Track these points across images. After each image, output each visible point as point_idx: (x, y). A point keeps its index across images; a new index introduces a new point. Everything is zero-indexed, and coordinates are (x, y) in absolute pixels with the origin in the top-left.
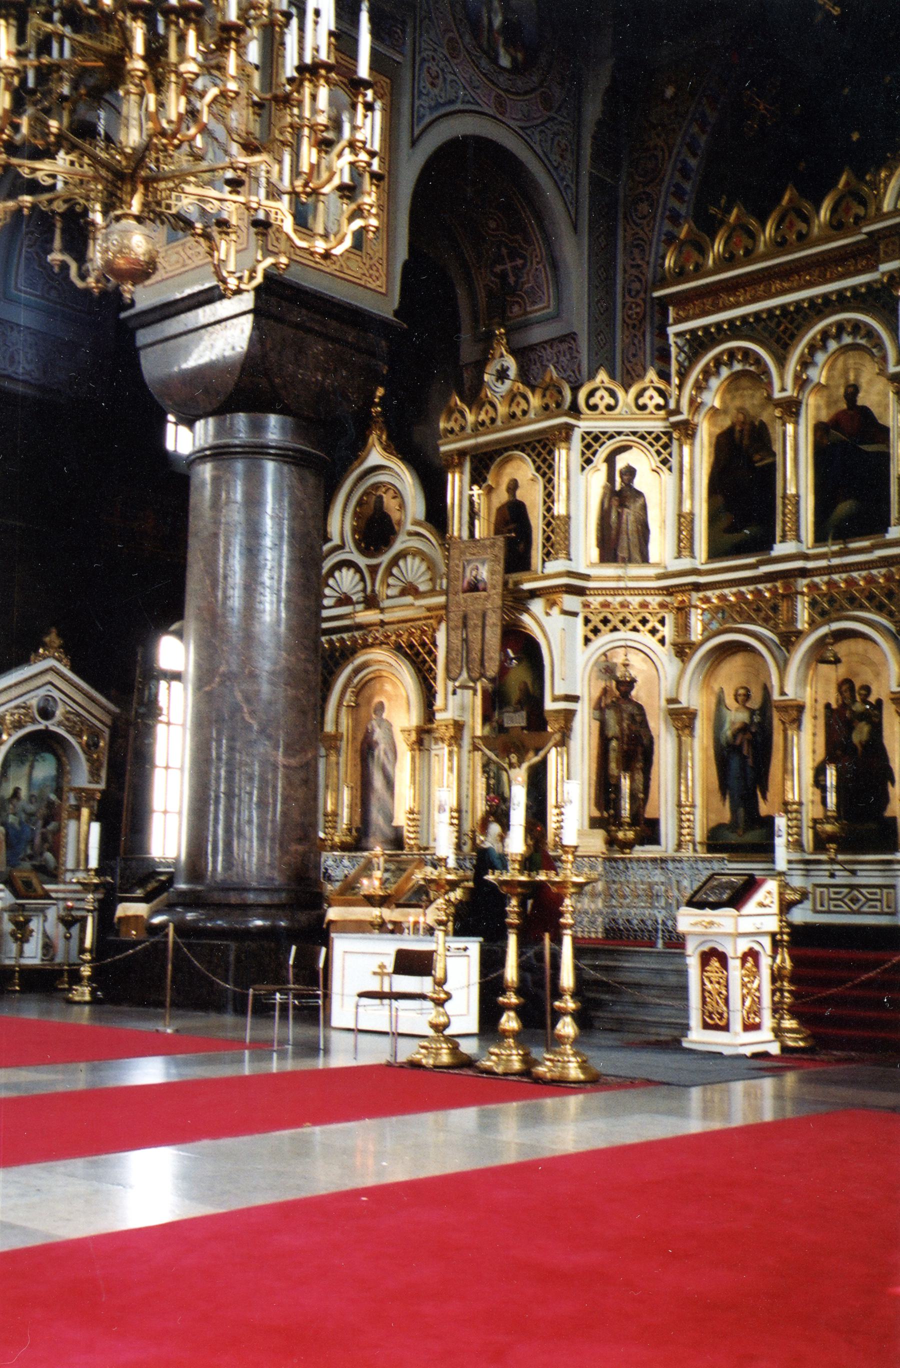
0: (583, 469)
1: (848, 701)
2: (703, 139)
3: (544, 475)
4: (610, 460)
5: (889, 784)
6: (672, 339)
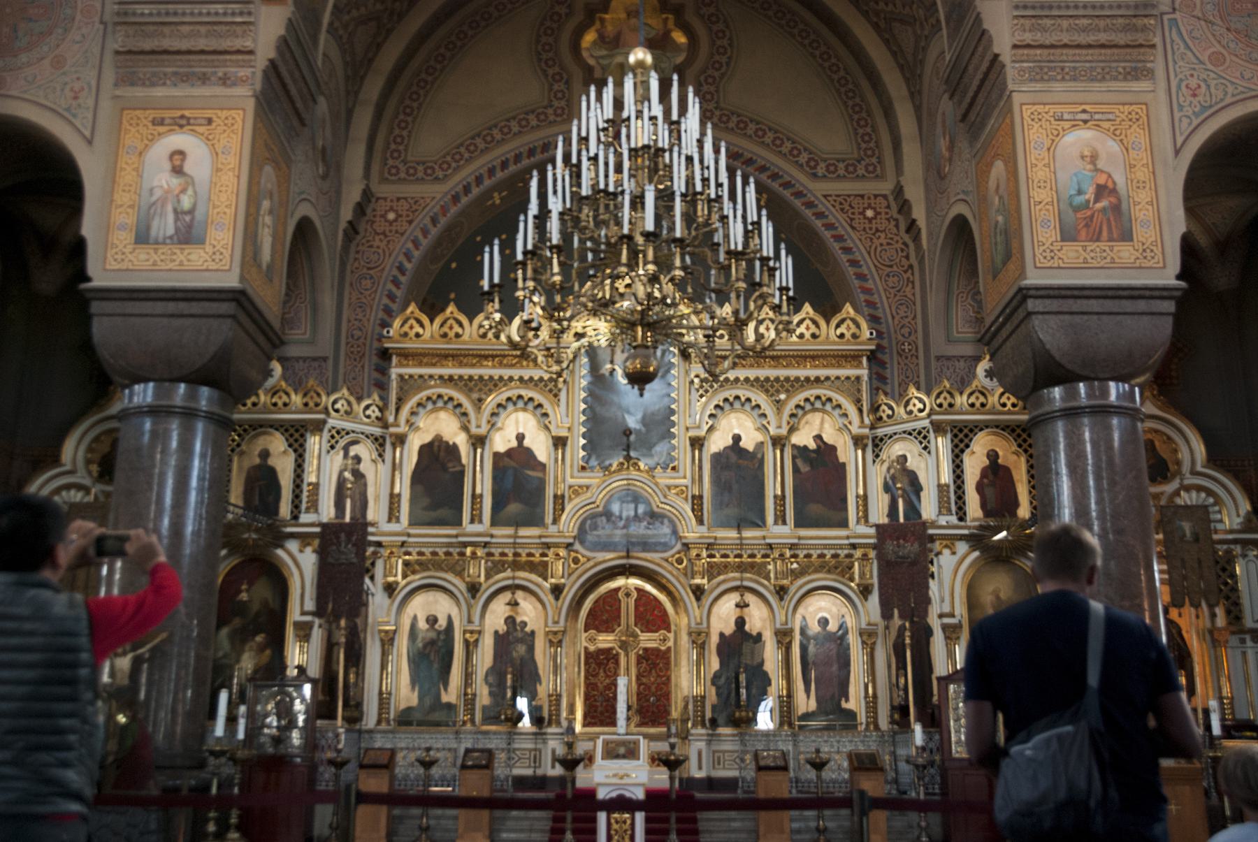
0: (328, 452)
1: (511, 630)
2: (416, 254)
3: (295, 451)
4: (346, 449)
5: (538, 685)
6: (394, 376)
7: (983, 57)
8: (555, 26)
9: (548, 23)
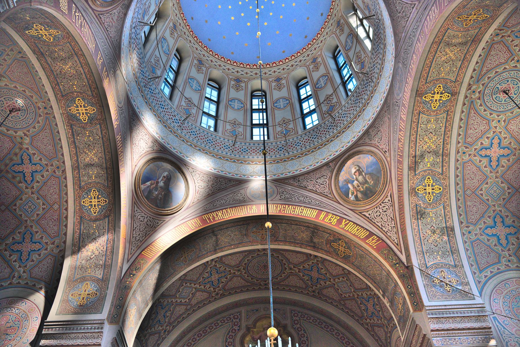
7: (419, 336)
8: (233, 334)
9: (231, 333)
